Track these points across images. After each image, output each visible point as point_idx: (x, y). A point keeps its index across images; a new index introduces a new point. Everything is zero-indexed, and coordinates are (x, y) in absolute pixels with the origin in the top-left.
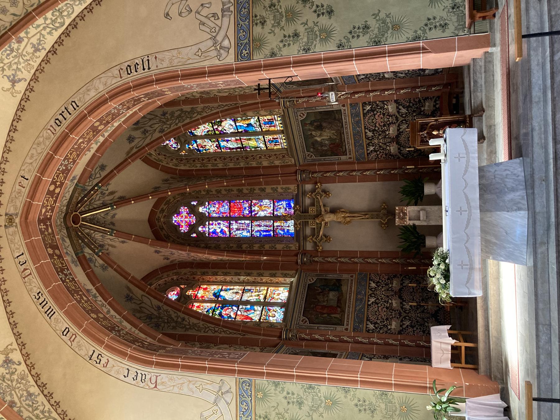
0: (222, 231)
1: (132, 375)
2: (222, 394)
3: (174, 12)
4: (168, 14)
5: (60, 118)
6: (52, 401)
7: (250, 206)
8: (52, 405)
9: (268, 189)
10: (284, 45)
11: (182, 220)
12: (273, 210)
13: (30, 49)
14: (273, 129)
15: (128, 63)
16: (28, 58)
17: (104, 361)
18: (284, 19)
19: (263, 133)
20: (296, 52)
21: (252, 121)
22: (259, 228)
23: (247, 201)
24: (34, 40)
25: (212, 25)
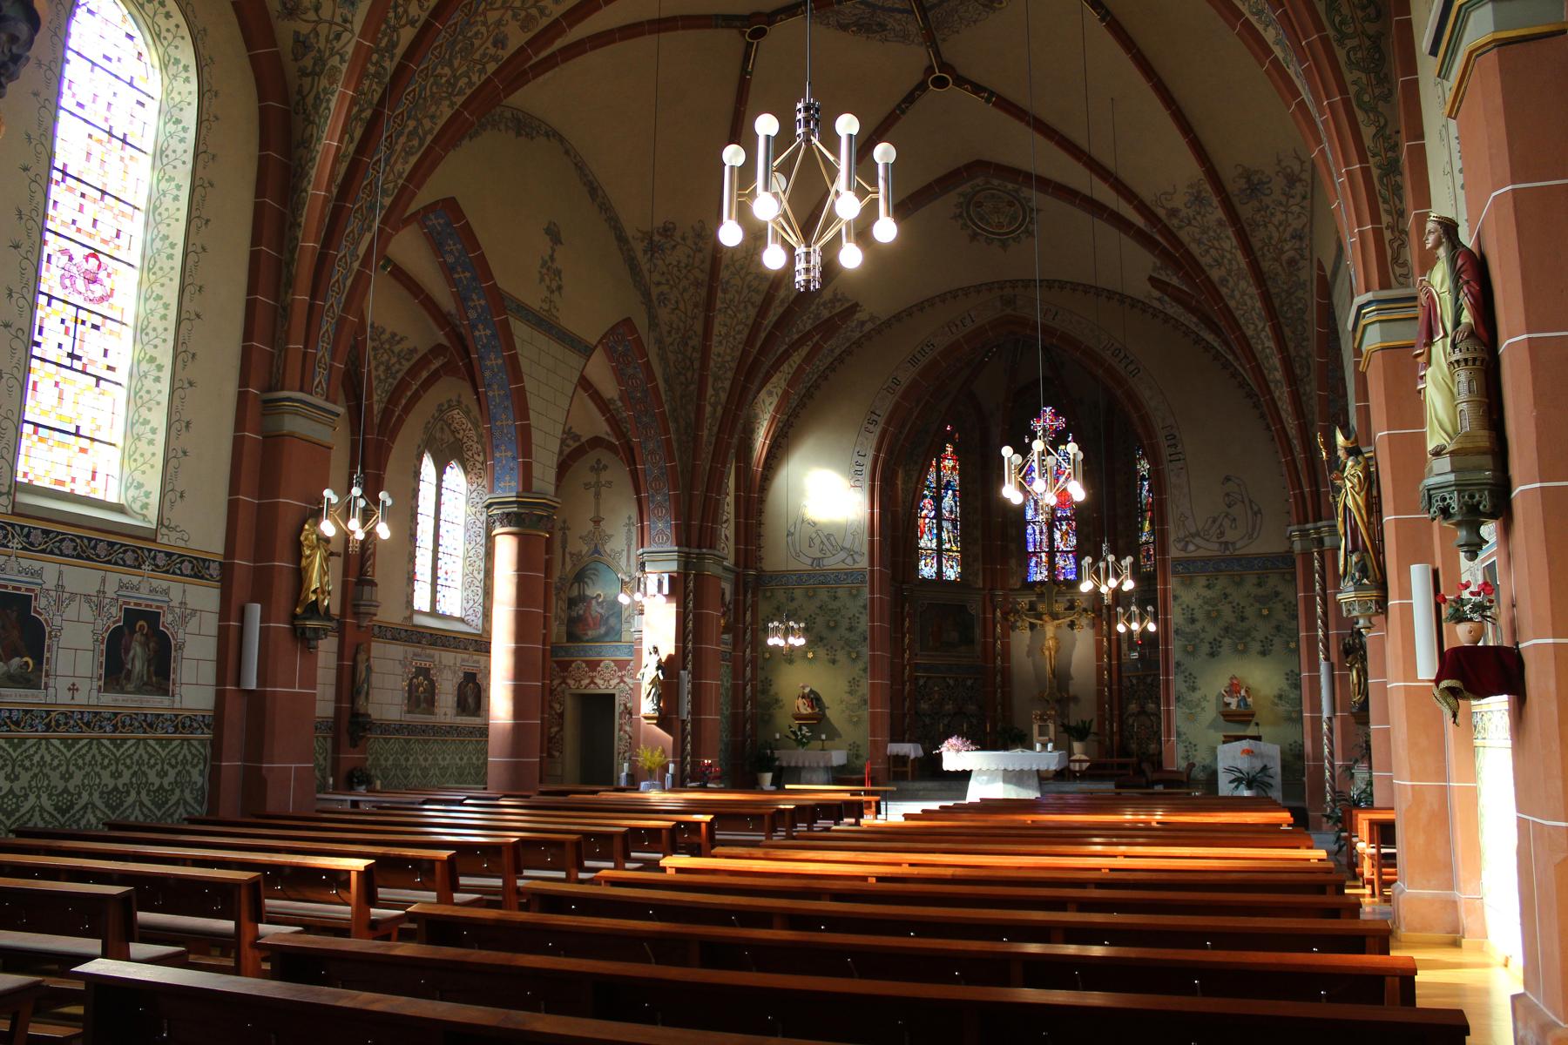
7: (1067, 518)
17: (871, 427)
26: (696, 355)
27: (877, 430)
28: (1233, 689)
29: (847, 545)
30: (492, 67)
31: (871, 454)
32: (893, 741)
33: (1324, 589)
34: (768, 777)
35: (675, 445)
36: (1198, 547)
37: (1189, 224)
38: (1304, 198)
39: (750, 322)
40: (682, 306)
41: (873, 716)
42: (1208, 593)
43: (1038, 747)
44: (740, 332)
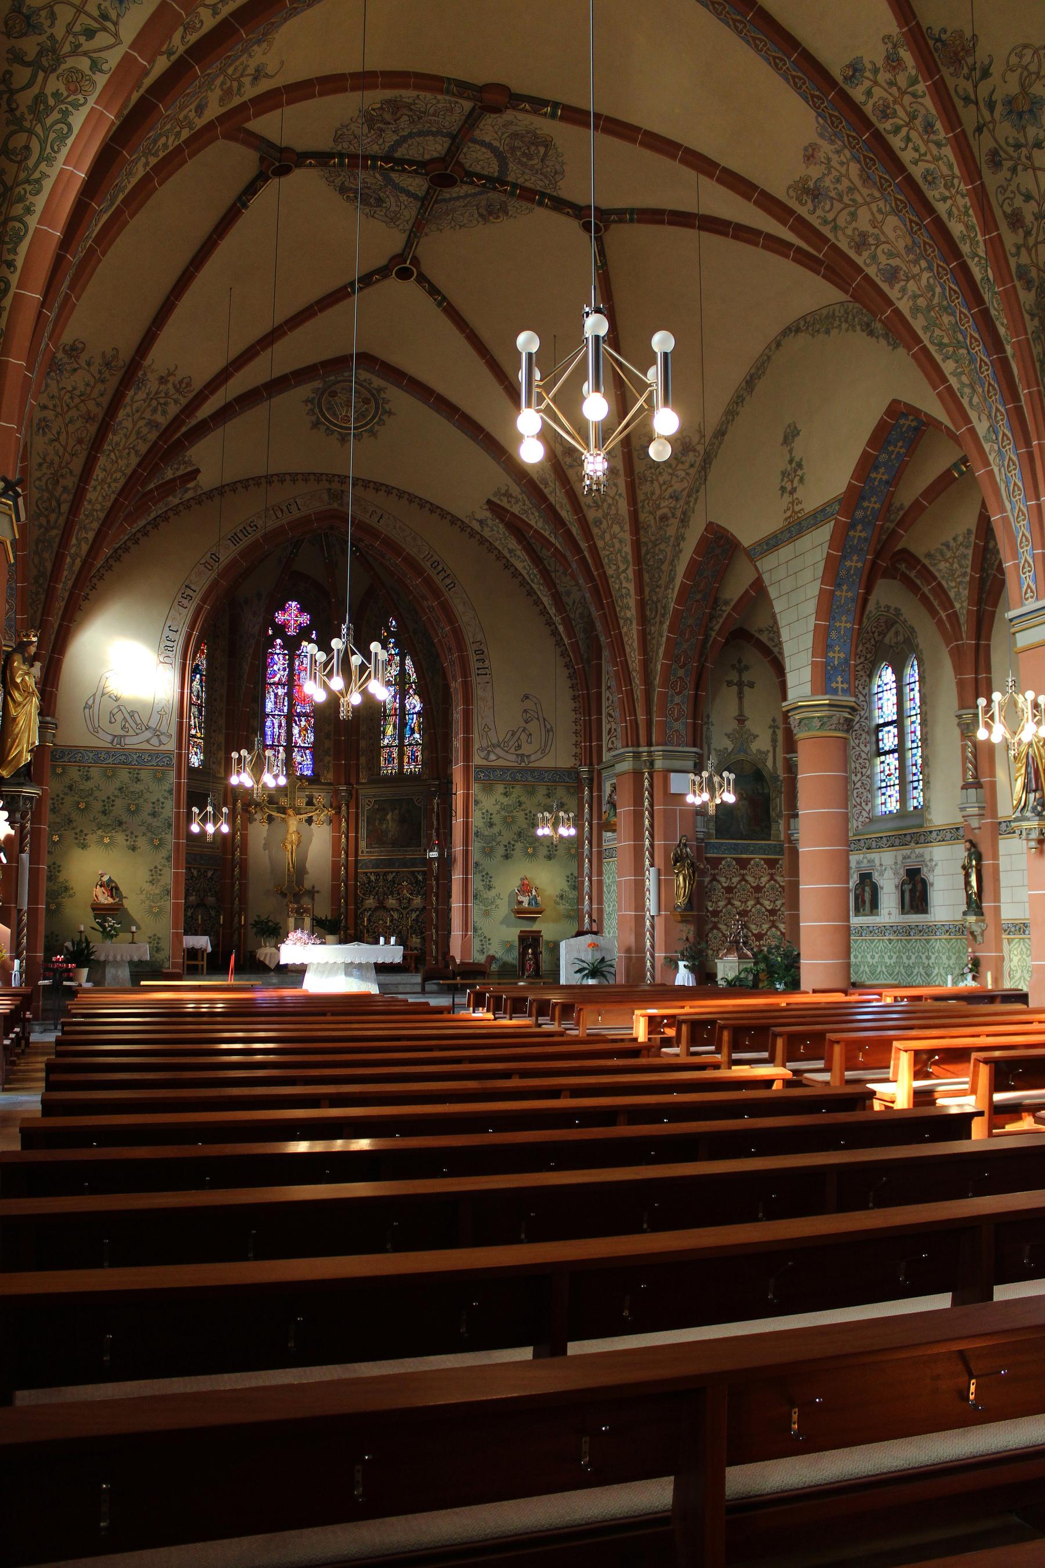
3: (528, 704)
4: (527, 698)
5: (440, 568)
6: (139, 535)
7: (306, 715)
9: (328, 744)
12: (300, 747)
13: (510, 546)
14: (406, 760)
17: (185, 602)
19: (401, 746)
21: (417, 736)
22: (276, 725)
23: (313, 711)
24: (518, 553)
25: (511, 744)
26: (67, 497)
27: (192, 606)
28: (525, 888)
29: (153, 724)
30: (185, 134)
31: (185, 629)
32: (186, 933)
33: (652, 805)
34: (85, 972)
36: (499, 757)
38: (692, 466)
40: (63, 437)
41: (176, 905)
42: (505, 801)
43: (382, 940)
44: (116, 480)
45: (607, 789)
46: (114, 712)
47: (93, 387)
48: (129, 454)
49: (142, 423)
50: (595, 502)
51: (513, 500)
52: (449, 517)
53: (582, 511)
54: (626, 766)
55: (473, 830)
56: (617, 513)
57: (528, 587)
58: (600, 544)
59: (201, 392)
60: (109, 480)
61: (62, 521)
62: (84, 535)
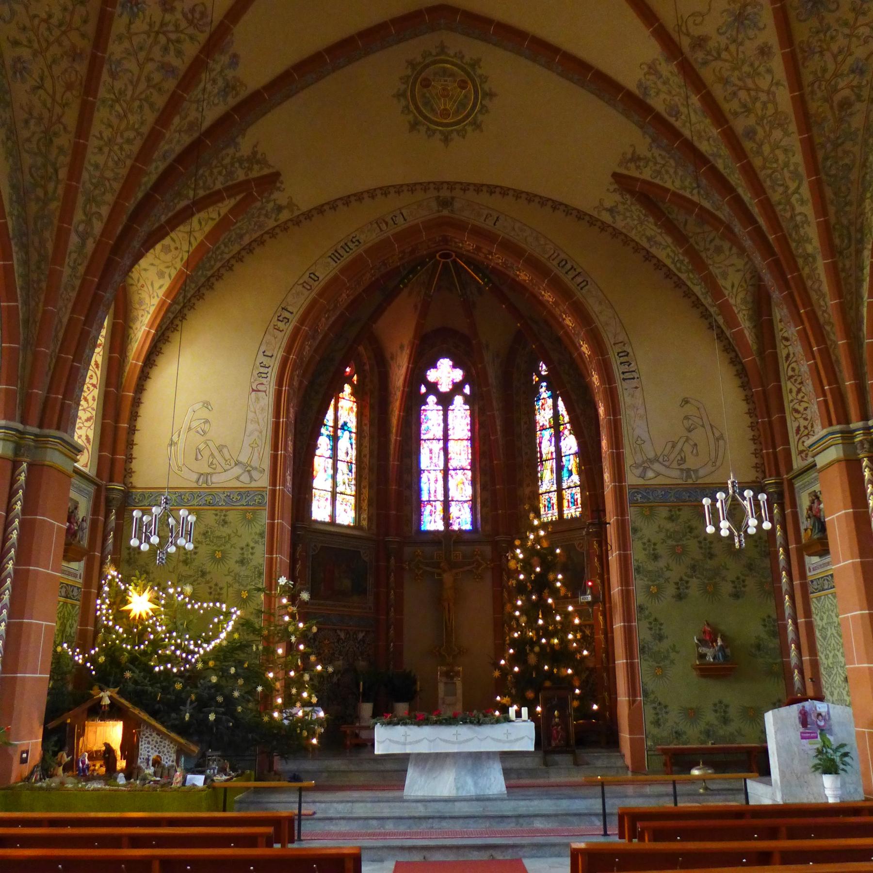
0: (428, 430)
1: (266, 361)
2: (249, 471)
3: (689, 409)
5: (568, 266)
6: (233, 262)
8: (228, 261)
10: (644, 544)
11: (445, 373)
13: (649, 233)
14: (565, 504)
15: (631, 354)
16: (639, 229)
18: (674, 543)
19: (560, 490)
20: (636, 557)
22: (432, 481)
24: (659, 238)
25: (672, 456)
27: (289, 329)
28: (709, 637)
31: (279, 354)
35: (19, 282)
36: (658, 474)
37: (718, 57)
39: (145, 130)
40: (48, 84)
42: (670, 526)
45: (804, 501)
46: (202, 446)
47: (72, 13)
48: (141, 107)
49: (150, 66)
50: (744, 106)
51: (642, 164)
52: (575, 213)
53: (727, 121)
54: (833, 454)
55: (633, 564)
56: (776, 112)
57: (675, 278)
58: (757, 162)
59: (222, 23)
60: (119, 140)
61: (60, 191)
62: (94, 209)
